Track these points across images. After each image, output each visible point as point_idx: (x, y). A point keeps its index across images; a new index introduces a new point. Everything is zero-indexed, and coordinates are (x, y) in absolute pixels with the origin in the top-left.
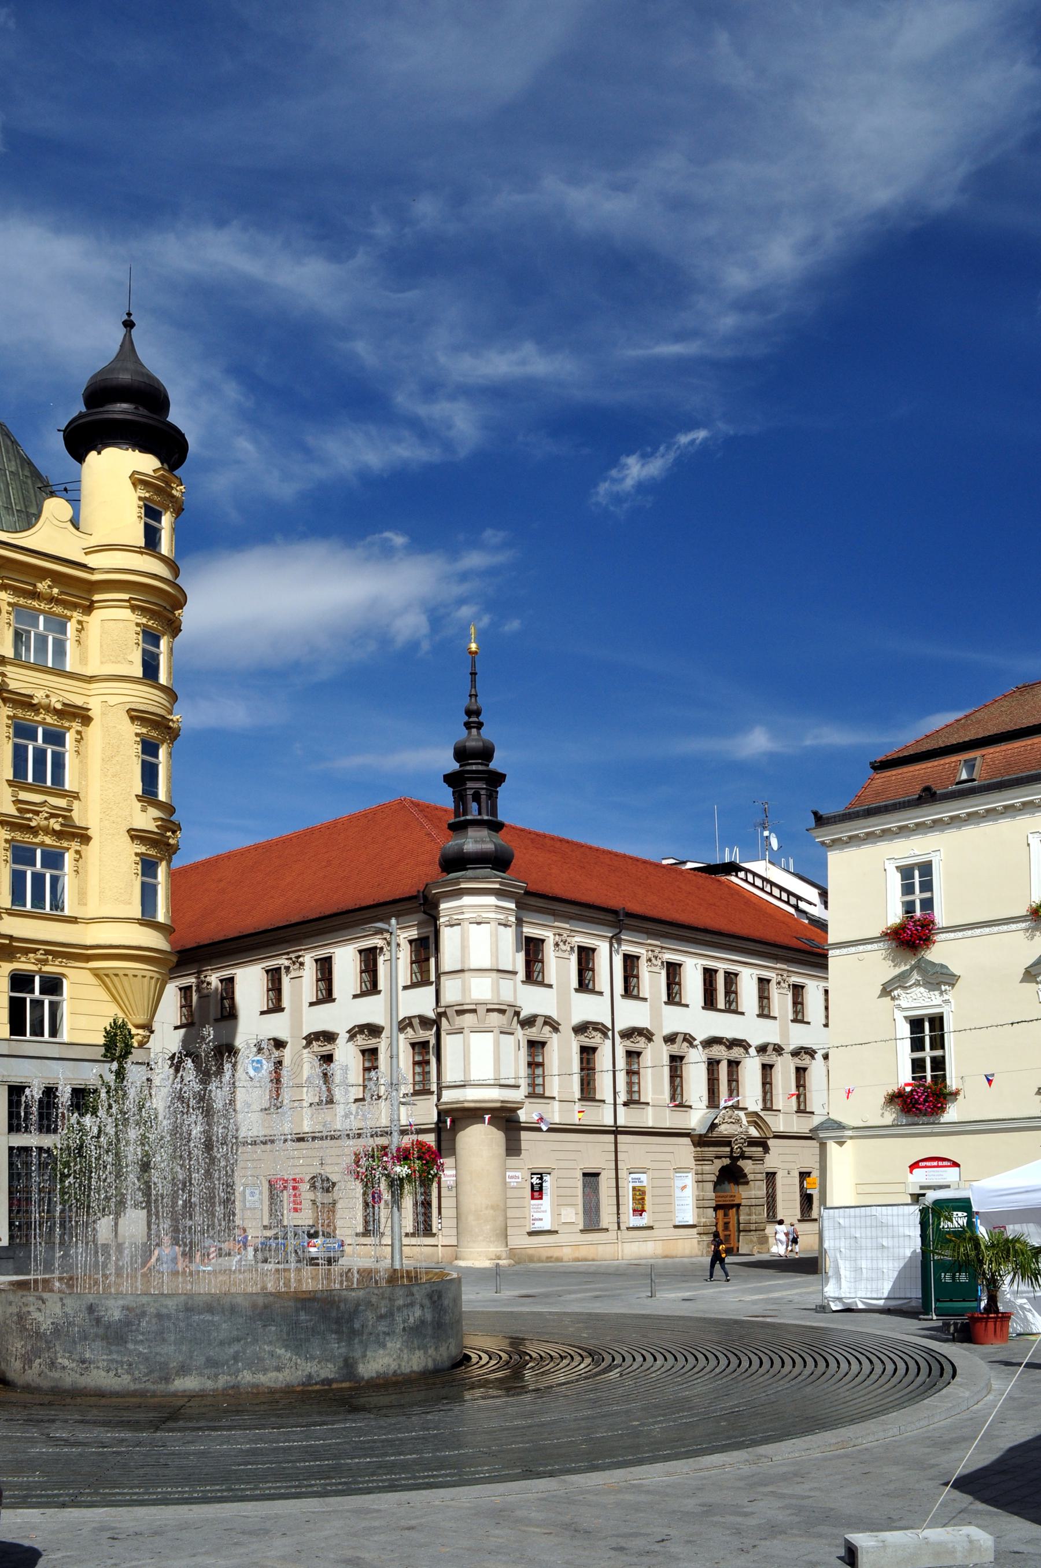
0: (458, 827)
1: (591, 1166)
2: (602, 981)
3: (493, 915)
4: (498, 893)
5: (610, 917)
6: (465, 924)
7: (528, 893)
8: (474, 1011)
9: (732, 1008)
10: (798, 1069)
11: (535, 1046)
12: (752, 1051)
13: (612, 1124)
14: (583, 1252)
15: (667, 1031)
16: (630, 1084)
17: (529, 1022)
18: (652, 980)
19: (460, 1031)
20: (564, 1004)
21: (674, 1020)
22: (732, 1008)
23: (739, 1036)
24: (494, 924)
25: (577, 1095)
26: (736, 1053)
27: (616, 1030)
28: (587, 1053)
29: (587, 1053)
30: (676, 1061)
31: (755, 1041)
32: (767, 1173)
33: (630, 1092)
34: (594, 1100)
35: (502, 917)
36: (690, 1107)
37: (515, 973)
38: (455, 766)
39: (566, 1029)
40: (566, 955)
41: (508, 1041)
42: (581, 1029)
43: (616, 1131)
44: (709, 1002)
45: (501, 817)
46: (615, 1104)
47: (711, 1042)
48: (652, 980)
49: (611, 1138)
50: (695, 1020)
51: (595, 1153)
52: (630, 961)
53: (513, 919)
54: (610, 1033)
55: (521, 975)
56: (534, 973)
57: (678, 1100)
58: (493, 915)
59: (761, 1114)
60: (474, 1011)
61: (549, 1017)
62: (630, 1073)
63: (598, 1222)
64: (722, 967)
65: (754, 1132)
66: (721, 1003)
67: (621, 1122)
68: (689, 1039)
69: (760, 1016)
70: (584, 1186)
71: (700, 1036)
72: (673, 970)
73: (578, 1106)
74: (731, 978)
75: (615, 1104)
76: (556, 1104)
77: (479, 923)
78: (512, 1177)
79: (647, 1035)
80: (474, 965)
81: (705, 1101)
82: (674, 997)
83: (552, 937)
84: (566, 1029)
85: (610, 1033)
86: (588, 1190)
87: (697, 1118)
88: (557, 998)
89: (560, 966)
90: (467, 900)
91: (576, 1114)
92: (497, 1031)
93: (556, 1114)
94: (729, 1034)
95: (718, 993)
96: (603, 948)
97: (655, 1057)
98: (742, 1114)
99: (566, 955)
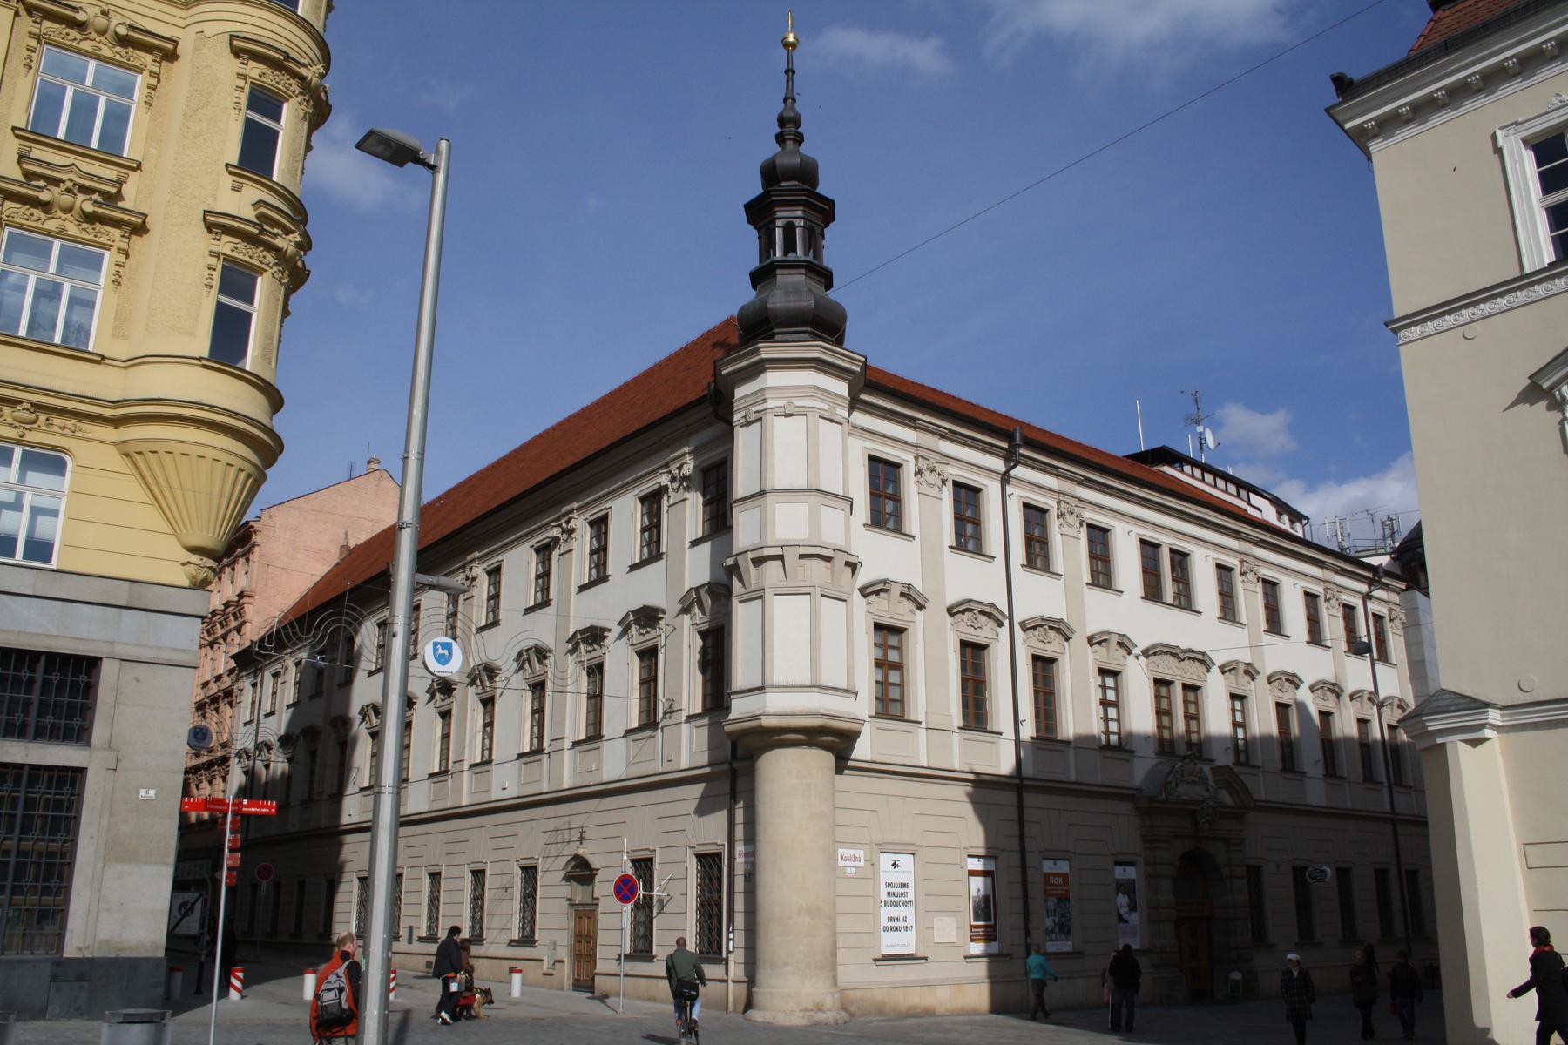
2: (993, 542)
8: (781, 558)
9: (1185, 601)
18: (1068, 547)
19: (759, 595)
22: (1185, 601)
25: (957, 719)
28: (973, 653)
31: (1219, 659)
32: (1249, 867)
36: (1132, 752)
39: (936, 609)
44: (1153, 592)
48: (1068, 547)
52: (1035, 515)
56: (886, 506)
59: (1237, 769)
60: (781, 558)
61: (909, 586)
64: (1166, 541)
65: (1227, 799)
66: (1169, 595)
71: (1142, 643)
73: (956, 738)
74: (1180, 559)
76: (922, 733)
77: (787, 415)
79: (1062, 630)
83: (912, 461)
84: (936, 609)
85: (1006, 622)
88: (918, 555)
89: (928, 509)
90: (772, 378)
95: (1165, 577)
96: (992, 489)
99: (934, 491)
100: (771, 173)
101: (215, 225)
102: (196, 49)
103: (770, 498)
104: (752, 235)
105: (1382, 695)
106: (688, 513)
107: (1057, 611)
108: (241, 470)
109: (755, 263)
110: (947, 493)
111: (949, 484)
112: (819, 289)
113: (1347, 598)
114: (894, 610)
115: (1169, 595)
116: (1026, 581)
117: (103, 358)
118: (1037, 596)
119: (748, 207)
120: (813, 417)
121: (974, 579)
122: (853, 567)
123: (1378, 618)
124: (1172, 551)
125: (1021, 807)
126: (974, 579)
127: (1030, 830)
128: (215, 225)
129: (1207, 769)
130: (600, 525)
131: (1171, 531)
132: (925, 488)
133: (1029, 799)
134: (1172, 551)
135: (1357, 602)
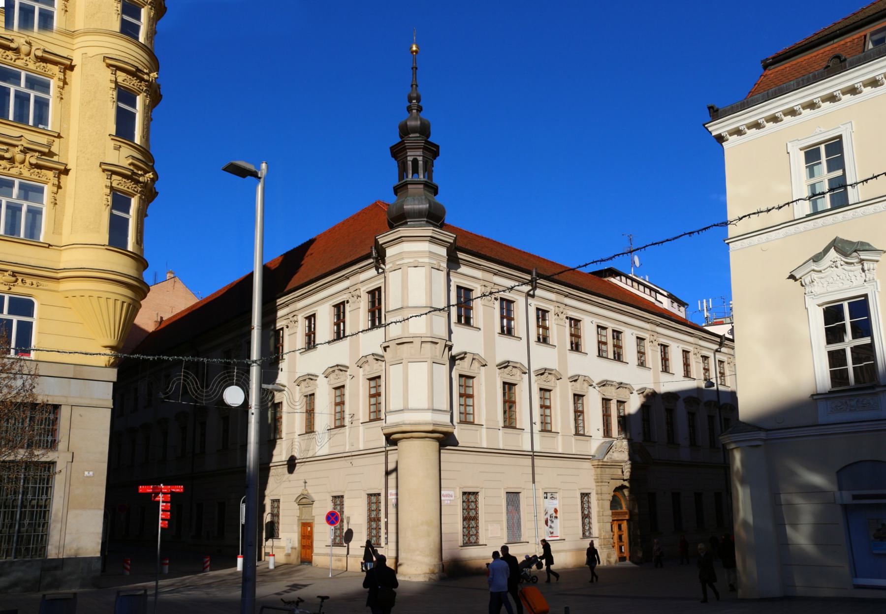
3: (427, 260)
4: (433, 240)
6: (404, 268)
12: (635, 393)
13: (530, 449)
16: (543, 416)
18: (559, 331)
20: (489, 345)
21: (576, 364)
22: (618, 357)
24: (428, 267)
25: (501, 424)
29: (509, 387)
33: (543, 423)
34: (515, 428)
35: (435, 262)
42: (504, 365)
43: (533, 455)
44: (601, 354)
45: (436, 180)
47: (604, 384)
48: (559, 331)
50: (591, 365)
51: (515, 474)
52: (542, 314)
58: (427, 260)
63: (520, 536)
70: (508, 505)
71: (596, 380)
73: (501, 433)
74: (617, 334)
76: (484, 431)
78: (446, 496)
81: (601, 433)
86: (510, 507)
89: (485, 312)
90: (406, 247)
91: (503, 439)
92: (430, 361)
93: (482, 438)
96: (520, 302)
99: (490, 304)
100: (405, 131)
101: (110, 171)
104: (394, 164)
105: (722, 402)
106: (358, 315)
108: (123, 302)
109: (396, 182)
110: (497, 304)
112: (431, 196)
113: (705, 353)
115: (611, 356)
116: (538, 349)
117: (50, 245)
118: (543, 357)
119: (392, 149)
121: (509, 349)
123: (721, 362)
124: (614, 331)
126: (509, 349)
128: (110, 171)
130: (311, 318)
131: (613, 318)
133: (537, 461)
134: (614, 331)
135: (711, 355)
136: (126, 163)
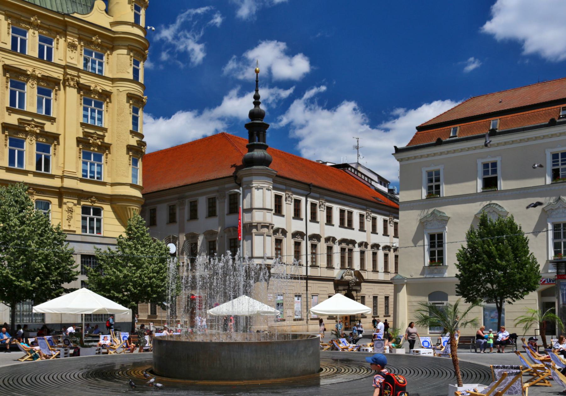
0: (251, 148)
1: (298, 292)
2: (303, 216)
5: (307, 187)
7: (277, 176)
9: (350, 226)
10: (373, 253)
11: (278, 242)
13: (305, 274)
14: (294, 328)
15: (326, 236)
16: (312, 258)
17: (276, 231)
18: (322, 215)
21: (328, 231)
22: (350, 226)
23: (353, 239)
26: (351, 246)
27: (308, 234)
28: (297, 244)
30: (330, 249)
31: (358, 241)
32: (362, 297)
33: (312, 262)
37: (271, 210)
38: (250, 121)
40: (289, 203)
41: (268, 238)
43: (307, 278)
44: (342, 225)
46: (307, 267)
48: (322, 215)
49: (305, 281)
53: (271, 187)
54: (305, 237)
55: (273, 212)
57: (330, 266)
62: (312, 253)
67: (309, 274)
68: (334, 239)
69: (360, 230)
71: (338, 238)
72: (329, 210)
74: (350, 213)
75: (307, 267)
80: (256, 207)
82: (329, 221)
85: (305, 237)
87: (336, 273)
89: (288, 208)
91: (293, 270)
94: (349, 237)
97: (322, 247)
98: (353, 272)
99: (289, 203)
102: (118, 95)
103: (254, 211)
107: (317, 232)
111: (293, 200)
114: (279, 236)
115: (346, 225)
120: (265, 189)
122: (272, 227)
125: (307, 283)
126: (298, 226)
127: (309, 288)
129: (353, 272)
132: (288, 202)
136: (135, 144)
